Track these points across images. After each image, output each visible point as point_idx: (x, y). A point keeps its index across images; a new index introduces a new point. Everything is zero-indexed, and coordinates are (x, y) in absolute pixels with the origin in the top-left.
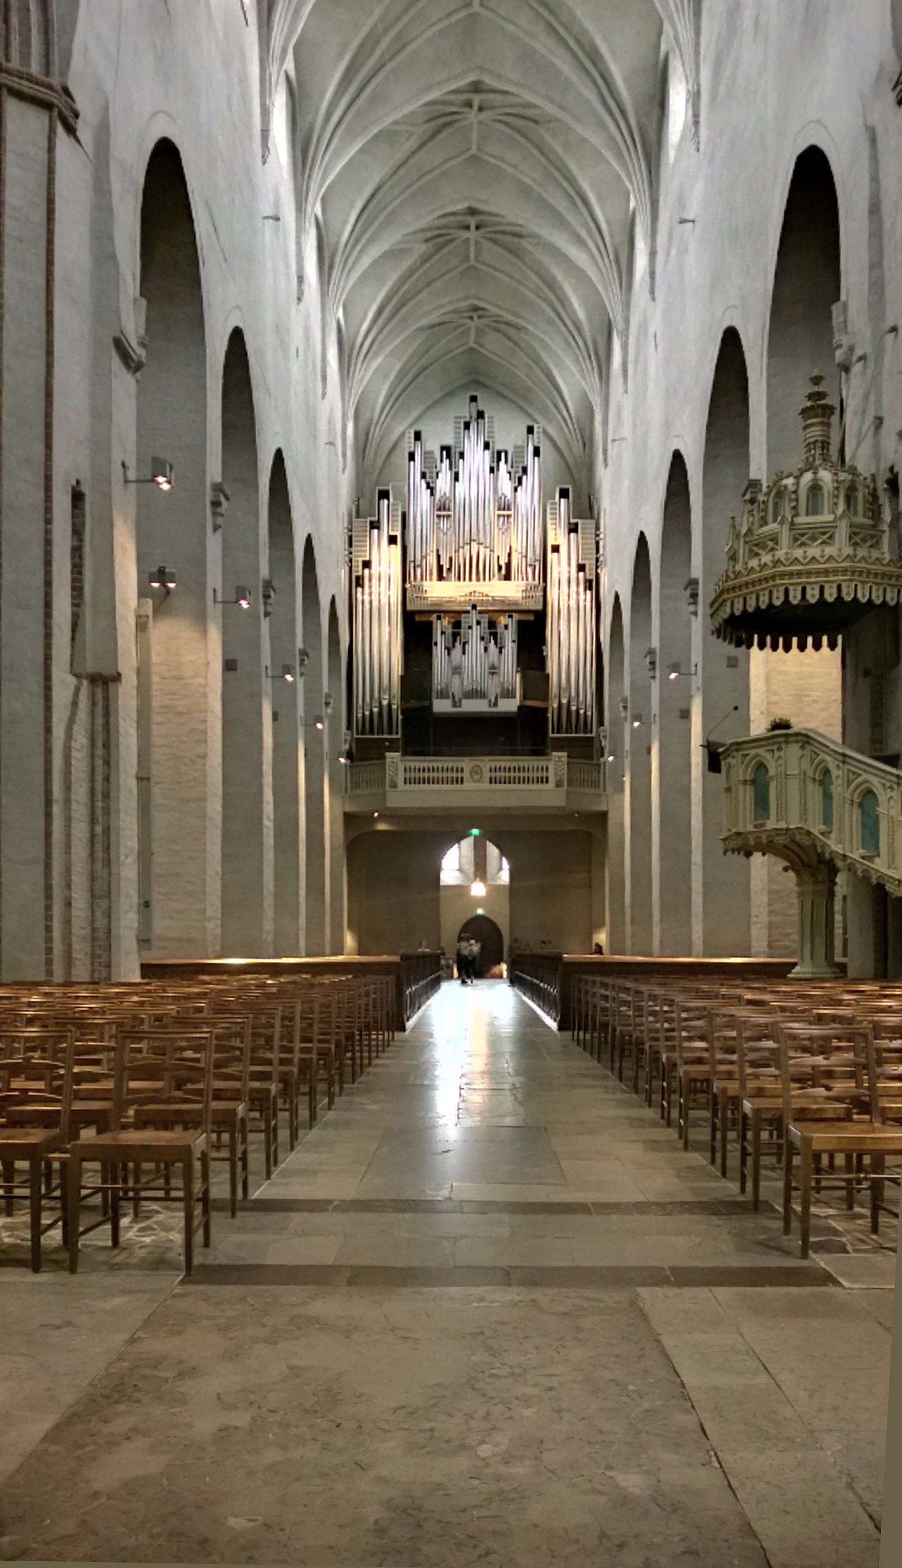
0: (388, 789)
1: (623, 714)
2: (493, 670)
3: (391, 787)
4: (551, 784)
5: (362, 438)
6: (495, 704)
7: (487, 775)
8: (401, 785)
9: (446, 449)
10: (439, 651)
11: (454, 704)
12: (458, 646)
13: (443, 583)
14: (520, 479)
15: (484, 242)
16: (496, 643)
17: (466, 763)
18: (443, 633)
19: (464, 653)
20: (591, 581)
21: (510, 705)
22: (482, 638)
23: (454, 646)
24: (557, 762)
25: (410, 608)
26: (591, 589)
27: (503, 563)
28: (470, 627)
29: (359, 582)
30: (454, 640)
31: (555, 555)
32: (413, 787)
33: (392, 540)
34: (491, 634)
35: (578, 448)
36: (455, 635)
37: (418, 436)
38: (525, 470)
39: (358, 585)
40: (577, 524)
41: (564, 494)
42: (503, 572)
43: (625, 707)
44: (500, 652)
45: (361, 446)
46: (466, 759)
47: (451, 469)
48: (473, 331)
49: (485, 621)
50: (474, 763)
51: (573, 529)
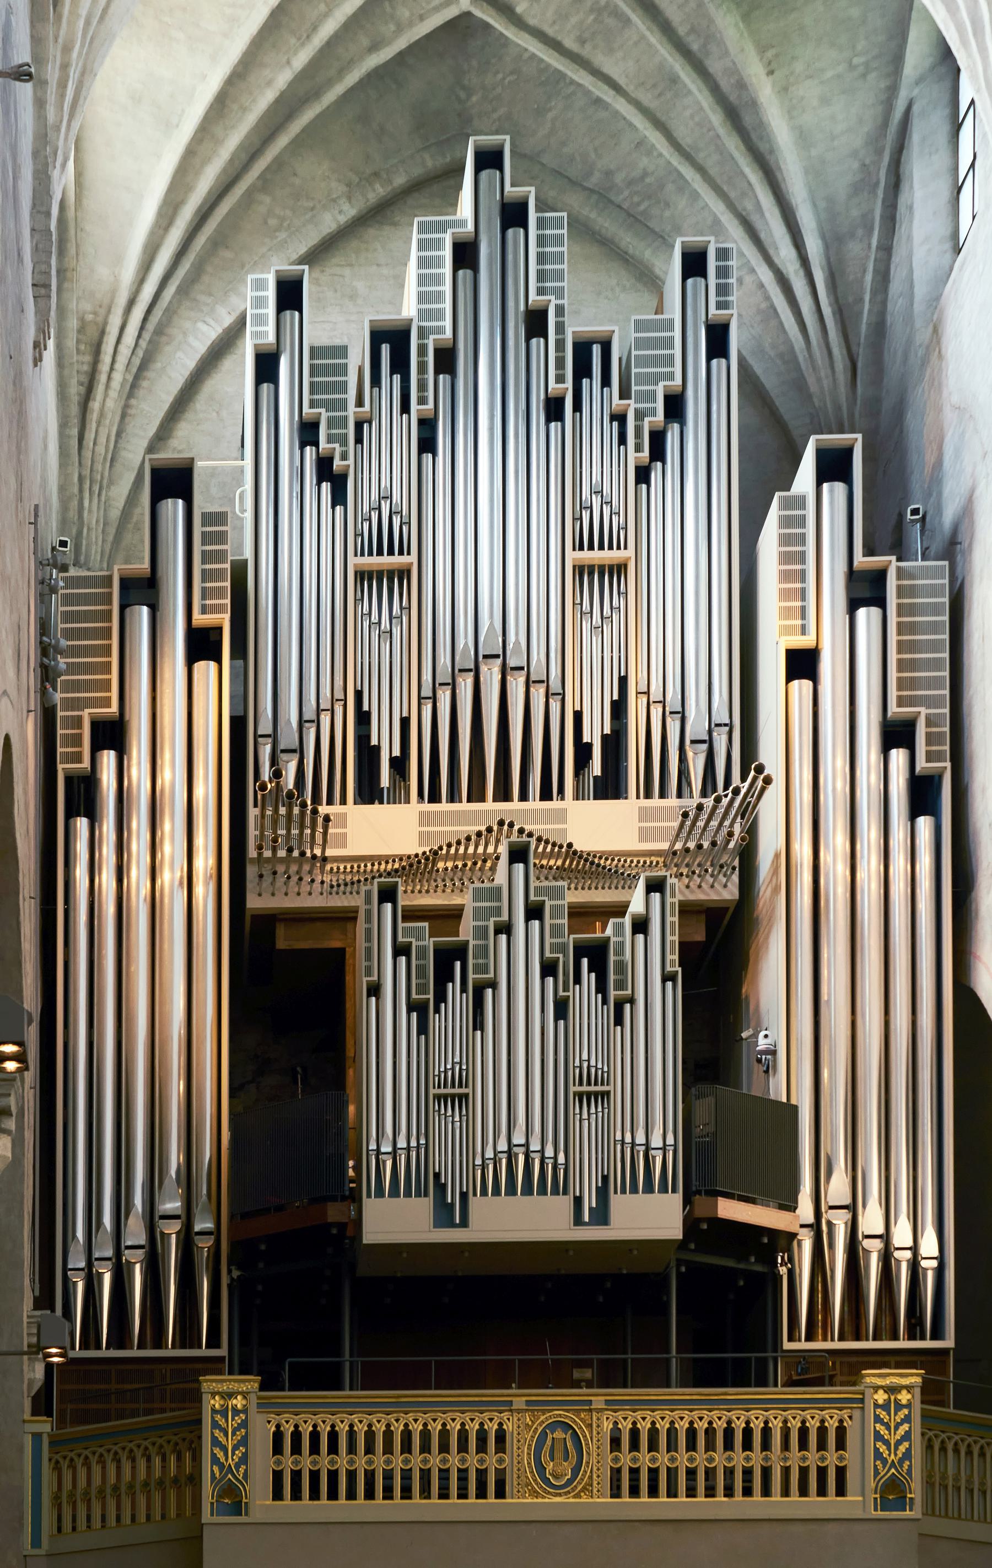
4: (858, 1502)
7: (599, 1460)
13: (374, 810)
14: (658, 440)
16: (602, 987)
17: (519, 1416)
18: (400, 950)
22: (549, 969)
23: (441, 997)
28: (505, 929)
30: (443, 976)
32: (307, 1509)
34: (581, 950)
36: (448, 958)
42: (596, 767)
44: (619, 1021)
46: (519, 1397)
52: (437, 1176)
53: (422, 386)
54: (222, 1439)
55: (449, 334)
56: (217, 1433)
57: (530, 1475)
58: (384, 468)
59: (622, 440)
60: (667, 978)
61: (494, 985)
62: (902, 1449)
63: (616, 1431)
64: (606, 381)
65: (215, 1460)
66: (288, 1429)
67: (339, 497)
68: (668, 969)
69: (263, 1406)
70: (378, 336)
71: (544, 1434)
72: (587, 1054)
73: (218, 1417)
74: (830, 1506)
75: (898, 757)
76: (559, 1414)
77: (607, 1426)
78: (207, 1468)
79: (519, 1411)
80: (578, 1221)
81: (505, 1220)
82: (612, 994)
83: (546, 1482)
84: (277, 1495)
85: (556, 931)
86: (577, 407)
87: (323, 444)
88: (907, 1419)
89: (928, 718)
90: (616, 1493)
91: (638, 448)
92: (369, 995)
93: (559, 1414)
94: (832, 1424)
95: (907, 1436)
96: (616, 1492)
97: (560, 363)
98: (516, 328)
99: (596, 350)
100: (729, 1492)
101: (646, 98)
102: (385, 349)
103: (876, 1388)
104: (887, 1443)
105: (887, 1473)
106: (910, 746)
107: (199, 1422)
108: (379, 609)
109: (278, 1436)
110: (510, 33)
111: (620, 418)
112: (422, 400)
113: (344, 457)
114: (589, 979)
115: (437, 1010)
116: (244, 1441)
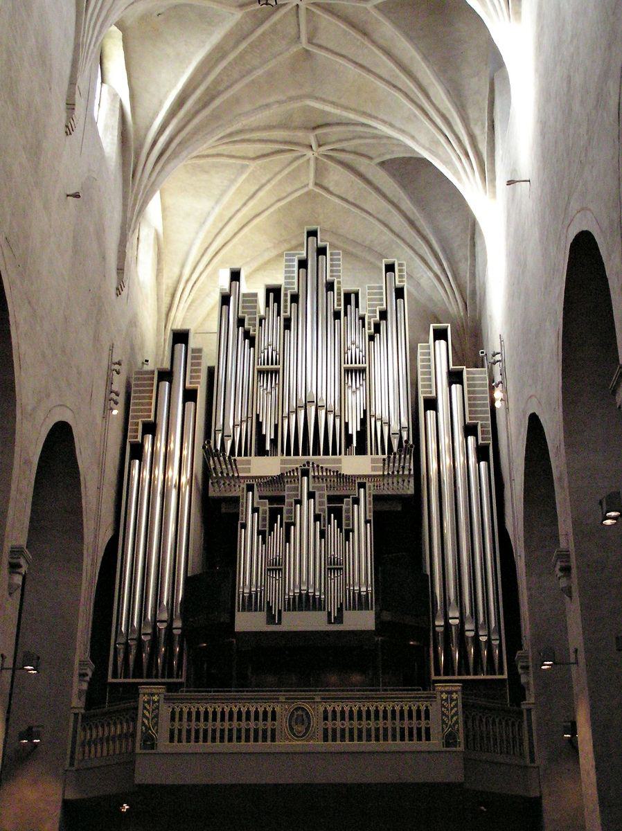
0: (138, 750)
1: (563, 583)
2: (334, 567)
3: (144, 747)
4: (436, 743)
5: (166, 300)
6: (339, 619)
8: (163, 745)
9: (274, 292)
10: (248, 540)
11: (271, 619)
12: (279, 530)
15: (317, 11)
16: (340, 525)
18: (255, 510)
19: (288, 540)
20: (486, 447)
21: (364, 620)
22: (317, 518)
23: (271, 529)
24: (445, 701)
25: (212, 493)
26: (487, 460)
27: (354, 429)
28: (299, 502)
29: (137, 451)
30: (273, 520)
31: (431, 413)
32: (185, 747)
33: (190, 395)
34: (330, 510)
35: (455, 307)
36: (274, 514)
37: (235, 276)
38: (383, 315)
39: (133, 457)
40: (460, 373)
41: (440, 334)
43: (566, 570)
44: (347, 538)
45: (164, 310)
47: (279, 314)
48: (312, 163)
49: (323, 494)
50: (294, 706)
51: (455, 377)
52: (268, 603)
53: (286, 307)
54: (147, 714)
55: (296, 290)
56: (145, 711)
57: (287, 731)
58: (269, 336)
59: (364, 326)
60: (367, 522)
61: (294, 524)
62: (455, 718)
63: (325, 711)
64: (357, 306)
65: (143, 723)
66: (178, 710)
67: (252, 345)
68: (368, 518)
69: (167, 699)
70: (269, 290)
71: (293, 713)
72: (335, 552)
73: (146, 705)
74: (423, 745)
75: (471, 439)
76: (300, 703)
77: (322, 709)
78: (139, 727)
79: (282, 702)
80: (330, 622)
81: (296, 622)
82: (344, 527)
83: (294, 734)
84: (172, 740)
85: (321, 503)
86: (346, 314)
87: (246, 326)
88: (456, 706)
89: (483, 422)
90: (325, 739)
91: (369, 329)
92: (241, 528)
93: (300, 703)
94: (423, 708)
95: (456, 714)
96: (326, 739)
97: (339, 300)
98: (322, 289)
99: (353, 296)
100: (377, 739)
101: (381, 217)
102: (272, 295)
103: (442, 692)
104: (447, 716)
105: (447, 730)
106: (476, 435)
107: (137, 709)
108: (264, 385)
109: (173, 713)
110: (328, 196)
111: (362, 318)
112: (285, 312)
113: (255, 331)
114: (334, 522)
115: (270, 535)
116: (157, 716)
